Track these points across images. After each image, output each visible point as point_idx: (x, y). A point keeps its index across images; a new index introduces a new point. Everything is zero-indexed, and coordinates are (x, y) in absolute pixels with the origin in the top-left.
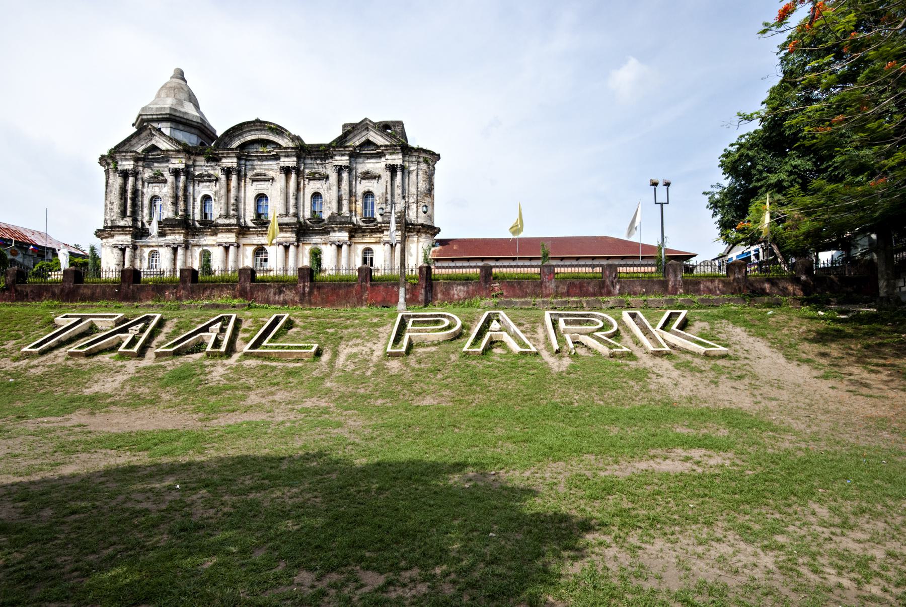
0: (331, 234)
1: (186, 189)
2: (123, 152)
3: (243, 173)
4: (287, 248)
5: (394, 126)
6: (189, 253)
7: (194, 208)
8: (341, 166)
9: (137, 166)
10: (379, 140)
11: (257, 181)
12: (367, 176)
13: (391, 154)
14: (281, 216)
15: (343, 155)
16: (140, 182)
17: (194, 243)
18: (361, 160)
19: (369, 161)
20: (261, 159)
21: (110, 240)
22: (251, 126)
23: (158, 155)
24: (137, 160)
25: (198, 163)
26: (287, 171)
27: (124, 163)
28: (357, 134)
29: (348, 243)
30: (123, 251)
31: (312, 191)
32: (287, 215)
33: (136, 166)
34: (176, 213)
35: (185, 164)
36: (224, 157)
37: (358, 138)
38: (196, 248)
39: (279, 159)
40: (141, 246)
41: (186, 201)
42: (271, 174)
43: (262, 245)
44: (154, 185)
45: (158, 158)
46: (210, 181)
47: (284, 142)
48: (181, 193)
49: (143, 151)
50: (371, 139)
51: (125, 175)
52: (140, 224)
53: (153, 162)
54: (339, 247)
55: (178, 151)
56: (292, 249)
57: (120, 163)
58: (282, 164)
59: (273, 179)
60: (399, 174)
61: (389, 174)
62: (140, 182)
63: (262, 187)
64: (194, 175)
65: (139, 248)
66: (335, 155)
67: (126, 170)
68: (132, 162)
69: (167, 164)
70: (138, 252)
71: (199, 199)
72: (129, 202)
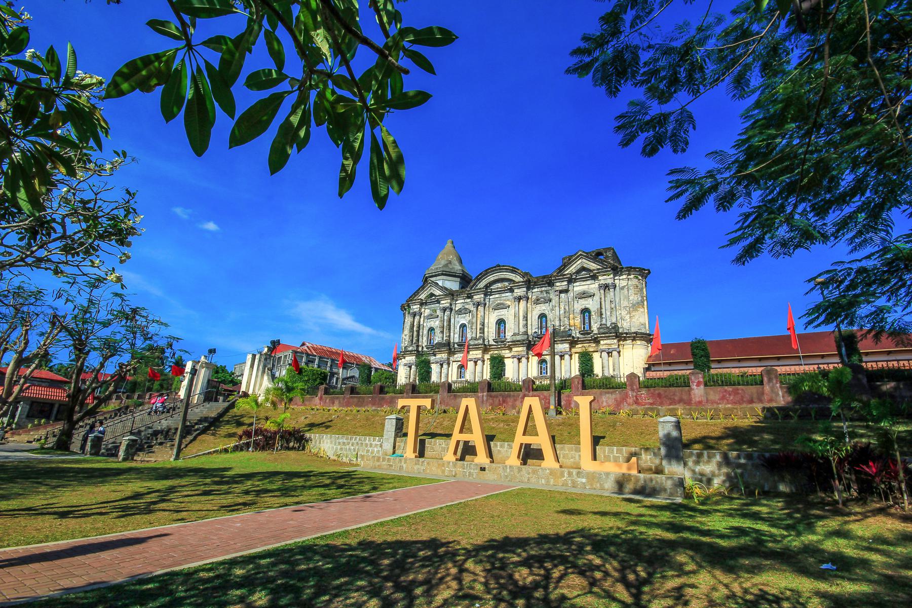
3: (487, 305)
5: (606, 252)
12: (584, 295)
14: (514, 335)
16: (422, 320)
19: (584, 283)
21: (403, 360)
26: (519, 299)
29: (569, 353)
30: (410, 367)
31: (539, 313)
32: (518, 334)
33: (420, 309)
41: (450, 329)
50: (585, 266)
56: (524, 360)
58: (515, 295)
61: (602, 291)
63: (503, 313)
72: (415, 333)
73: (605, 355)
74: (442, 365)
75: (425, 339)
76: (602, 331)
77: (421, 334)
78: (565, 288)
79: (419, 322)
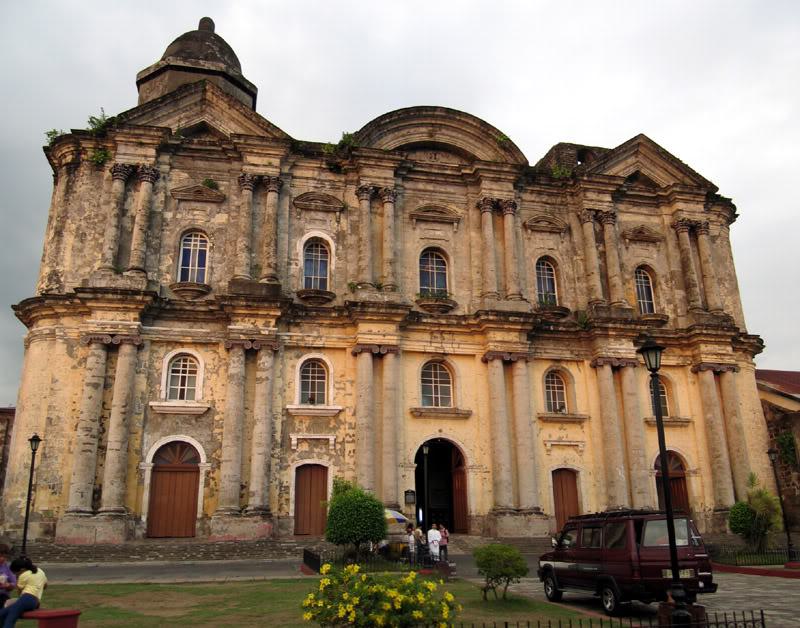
0: (600, 342)
2: (138, 127)
3: (400, 203)
4: (508, 364)
7: (289, 264)
8: (597, 211)
10: (662, 178)
11: (425, 221)
12: (641, 236)
13: (686, 201)
15: (601, 192)
17: (294, 342)
19: (635, 209)
20: (431, 177)
21: (66, 321)
22: (425, 117)
23: (213, 144)
24: (162, 149)
25: (298, 173)
26: (498, 208)
28: (621, 161)
30: (111, 349)
31: (540, 253)
33: (157, 162)
34: (255, 268)
36: (370, 166)
37: (621, 166)
38: (292, 354)
39: (477, 183)
40: (153, 342)
42: (460, 212)
43: (445, 354)
45: (210, 152)
46: (327, 211)
47: (483, 153)
49: (180, 131)
50: (642, 171)
51: (132, 176)
54: (617, 370)
56: (520, 366)
58: (485, 193)
59: (458, 221)
60: (703, 238)
61: (685, 236)
62: (161, 197)
63: (439, 234)
64: (291, 196)
65: (146, 348)
66: (586, 190)
67: (135, 168)
68: (152, 152)
69: (236, 165)
70: (145, 356)
71: (300, 248)
73: (709, 376)
74: (251, 355)
76: (703, 321)
77: (154, 242)
78: (605, 207)
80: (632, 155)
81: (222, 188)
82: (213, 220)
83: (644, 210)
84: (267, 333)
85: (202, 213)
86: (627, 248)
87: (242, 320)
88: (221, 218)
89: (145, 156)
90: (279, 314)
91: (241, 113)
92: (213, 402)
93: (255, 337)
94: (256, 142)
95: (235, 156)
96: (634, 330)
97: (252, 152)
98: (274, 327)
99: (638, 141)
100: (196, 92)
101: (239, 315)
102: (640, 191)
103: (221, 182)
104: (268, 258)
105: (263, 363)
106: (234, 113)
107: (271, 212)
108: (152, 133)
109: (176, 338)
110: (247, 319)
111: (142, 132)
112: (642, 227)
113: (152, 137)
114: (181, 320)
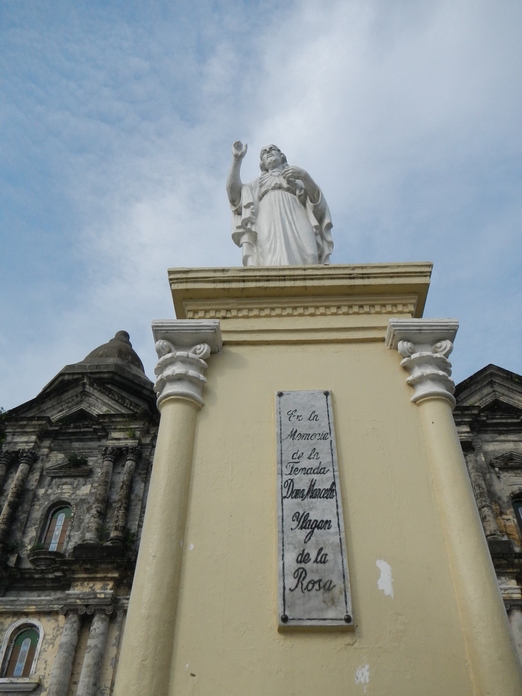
1: (130, 486)
2: (23, 419)
6: (115, 633)
9: (39, 447)
16: (36, 476)
18: (487, 437)
19: (502, 438)
24: (42, 435)
27: (18, 439)
28: (476, 392)
33: (37, 446)
35: (140, 440)
41: (128, 509)
44: (64, 480)
45: (84, 433)
48: (117, 496)
49: (60, 420)
50: (502, 399)
52: (13, 560)
53: (71, 441)
55: (133, 417)
57: (9, 439)
62: (36, 476)
67: (18, 451)
68: (33, 438)
75: (32, 533)
77: (23, 516)
79: (24, 480)
80: (485, 386)
81: (91, 463)
82: (78, 492)
83: (511, 437)
84: (103, 596)
85: (69, 487)
86: (499, 477)
87: (82, 585)
88: (85, 490)
89: (26, 442)
90: (116, 575)
91: (110, 398)
92: (44, 677)
93: (91, 602)
94: (118, 420)
95: (104, 434)
96: (512, 565)
97: (115, 429)
98: (110, 589)
99: (487, 373)
100: (77, 386)
101: (78, 579)
102: (501, 418)
103: (91, 458)
104: (116, 522)
105: (95, 629)
106: (106, 400)
107: (125, 479)
108: (34, 422)
109: (18, 608)
110: (86, 583)
111: (25, 423)
112: (511, 455)
113: (34, 426)
114: (31, 589)
